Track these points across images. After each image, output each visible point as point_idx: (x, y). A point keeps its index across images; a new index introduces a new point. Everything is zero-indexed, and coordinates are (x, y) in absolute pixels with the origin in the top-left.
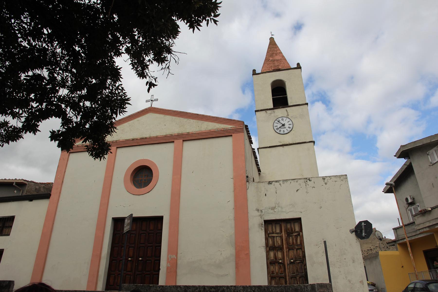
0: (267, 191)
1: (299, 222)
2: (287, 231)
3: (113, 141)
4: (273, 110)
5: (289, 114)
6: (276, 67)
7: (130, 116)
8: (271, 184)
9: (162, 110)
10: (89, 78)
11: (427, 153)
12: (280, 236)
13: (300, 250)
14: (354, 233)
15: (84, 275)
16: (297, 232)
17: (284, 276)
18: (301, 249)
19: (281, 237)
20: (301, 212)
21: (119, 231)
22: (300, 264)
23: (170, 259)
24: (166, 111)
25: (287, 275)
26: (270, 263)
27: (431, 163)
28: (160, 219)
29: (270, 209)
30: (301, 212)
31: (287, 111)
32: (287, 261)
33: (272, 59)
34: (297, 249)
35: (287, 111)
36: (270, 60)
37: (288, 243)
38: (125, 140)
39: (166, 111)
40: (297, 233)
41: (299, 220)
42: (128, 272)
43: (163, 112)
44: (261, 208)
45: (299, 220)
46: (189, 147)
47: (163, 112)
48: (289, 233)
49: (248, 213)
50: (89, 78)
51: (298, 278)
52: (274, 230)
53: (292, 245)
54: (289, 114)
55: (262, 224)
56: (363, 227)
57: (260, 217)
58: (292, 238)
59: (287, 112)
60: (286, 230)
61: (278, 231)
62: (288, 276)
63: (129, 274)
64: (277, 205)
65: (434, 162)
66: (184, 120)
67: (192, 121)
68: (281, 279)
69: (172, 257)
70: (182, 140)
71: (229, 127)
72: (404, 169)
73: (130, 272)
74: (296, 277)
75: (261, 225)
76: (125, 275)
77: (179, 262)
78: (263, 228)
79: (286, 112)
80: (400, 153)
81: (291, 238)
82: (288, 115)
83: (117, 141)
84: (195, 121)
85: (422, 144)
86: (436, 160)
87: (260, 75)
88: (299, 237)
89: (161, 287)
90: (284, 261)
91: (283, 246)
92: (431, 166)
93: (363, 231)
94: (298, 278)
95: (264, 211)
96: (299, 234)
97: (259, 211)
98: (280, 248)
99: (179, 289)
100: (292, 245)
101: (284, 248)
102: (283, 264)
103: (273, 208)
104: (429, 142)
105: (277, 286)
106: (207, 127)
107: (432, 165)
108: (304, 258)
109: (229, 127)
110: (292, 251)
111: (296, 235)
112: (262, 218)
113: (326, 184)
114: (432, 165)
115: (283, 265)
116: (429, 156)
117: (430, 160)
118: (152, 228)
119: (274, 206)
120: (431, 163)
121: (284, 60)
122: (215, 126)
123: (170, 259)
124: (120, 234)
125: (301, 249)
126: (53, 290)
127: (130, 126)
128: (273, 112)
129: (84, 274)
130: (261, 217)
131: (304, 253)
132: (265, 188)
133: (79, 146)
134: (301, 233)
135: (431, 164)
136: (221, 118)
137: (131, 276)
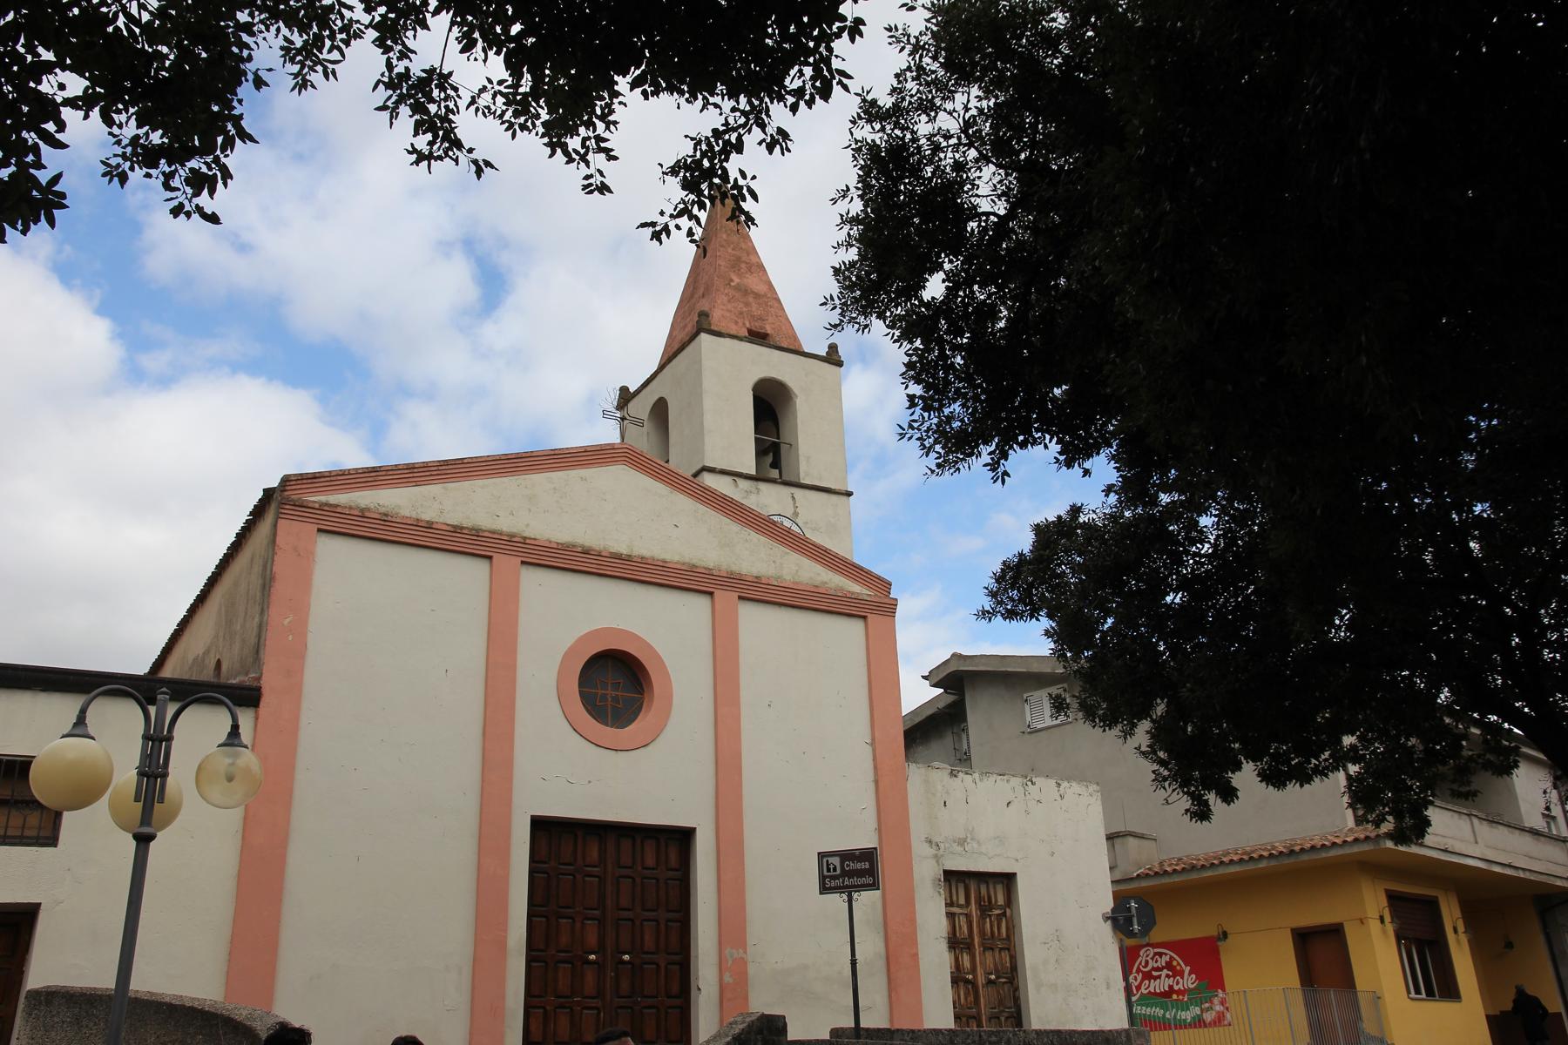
0: (947, 793)
1: (1005, 882)
2: (980, 905)
3: (514, 536)
4: (755, 483)
5: (798, 510)
6: (756, 324)
7: (556, 452)
8: (956, 776)
9: (665, 470)
10: (196, 137)
11: (1022, 697)
12: (966, 914)
13: (1007, 952)
14: (1109, 922)
15: (448, 1010)
16: (999, 907)
17: (976, 1015)
18: (1009, 949)
19: (968, 916)
20: (1017, 860)
21: (545, 863)
22: (1006, 987)
23: (730, 962)
24: (676, 476)
25: (983, 1012)
26: (957, 979)
27: (1029, 726)
28: (683, 837)
29: (955, 842)
30: (1017, 860)
31: (793, 498)
32: (981, 980)
33: (739, 281)
34: (1001, 949)
35: (793, 498)
36: (732, 284)
37: (982, 933)
38: (558, 543)
39: (676, 476)
40: (1001, 909)
41: (1008, 879)
42: (587, 997)
43: (669, 476)
44: (936, 839)
45: (1008, 879)
46: (755, 622)
47: (669, 476)
48: (985, 908)
49: (910, 847)
50: (196, 137)
51: (1003, 1019)
52: (955, 898)
53: (989, 939)
54: (798, 510)
55: (940, 880)
56: (1134, 911)
57: (934, 862)
58: (990, 920)
59: (795, 503)
60: (979, 899)
61: (962, 901)
62: (985, 1014)
63: (594, 1005)
64: (969, 835)
65: (1039, 727)
66: (732, 528)
67: (755, 537)
68: (970, 1021)
69: (735, 956)
70: (738, 594)
71: (855, 588)
72: (924, 717)
73: (593, 998)
74: (998, 1018)
75: (937, 882)
76: (579, 1008)
77: (752, 969)
78: (941, 890)
79: (792, 502)
80: (945, 674)
81: (988, 920)
82: (796, 514)
83: (528, 541)
84: (763, 539)
85: (1025, 670)
86: (1046, 720)
87: (723, 339)
88: (1004, 920)
89: (911, 1034)
90: (975, 977)
91: (973, 940)
92: (1027, 736)
93: (1135, 920)
94: (1003, 1019)
95: (942, 845)
96: (1004, 914)
97: (933, 846)
98: (967, 944)
99: (940, 1037)
100: (989, 939)
101: (974, 946)
102: (973, 983)
103: (962, 842)
104: (1049, 671)
105: (997, 1031)
106: (797, 571)
107: (1030, 733)
108: (1015, 974)
109: (855, 588)
110: (991, 953)
111: (998, 915)
112: (939, 865)
113: (1062, 797)
114: (1030, 733)
115: (972, 987)
116: (1027, 707)
117: (1028, 719)
118: (650, 860)
119: (962, 836)
120: (1029, 726)
121: (774, 301)
122: (819, 574)
123: (730, 962)
124: (548, 873)
125: (1009, 949)
126: (1527, 994)
127: (555, 489)
128: (753, 490)
129: (448, 1008)
130: (937, 862)
131: (1014, 960)
132: (943, 786)
133: (367, 514)
134: (1008, 910)
135: (1029, 730)
136: (836, 556)
137: (599, 1013)
